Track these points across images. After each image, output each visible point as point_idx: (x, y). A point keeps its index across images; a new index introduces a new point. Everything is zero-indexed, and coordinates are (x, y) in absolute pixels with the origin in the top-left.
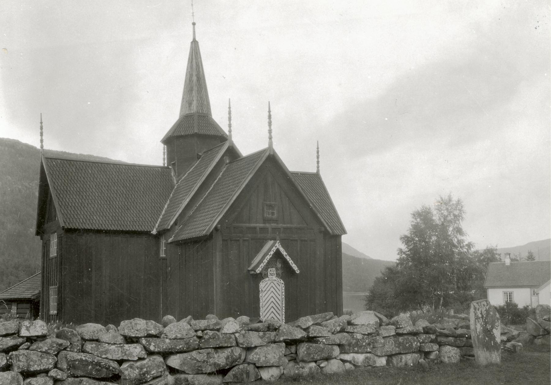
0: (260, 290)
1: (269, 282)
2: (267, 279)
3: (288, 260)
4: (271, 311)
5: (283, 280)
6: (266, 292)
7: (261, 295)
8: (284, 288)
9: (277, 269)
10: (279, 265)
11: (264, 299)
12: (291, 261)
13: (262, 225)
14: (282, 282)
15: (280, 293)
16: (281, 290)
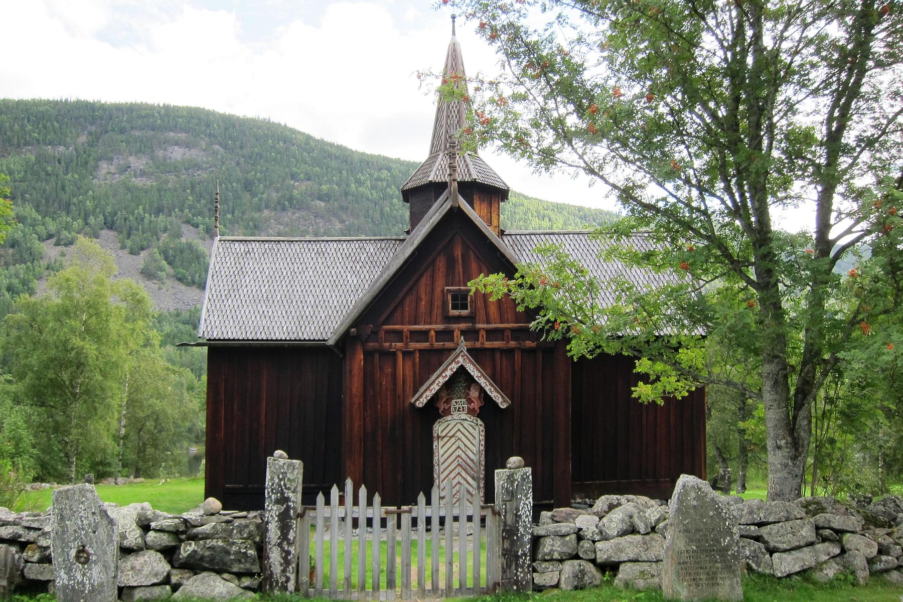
0: (435, 435)
1: (453, 423)
2: (449, 418)
3: (483, 385)
4: (457, 471)
5: (482, 420)
6: (446, 439)
7: (435, 443)
8: (483, 434)
9: (470, 401)
10: (474, 393)
11: (441, 452)
12: (490, 387)
13: (440, 327)
14: (480, 422)
15: (476, 442)
16: (477, 437)
